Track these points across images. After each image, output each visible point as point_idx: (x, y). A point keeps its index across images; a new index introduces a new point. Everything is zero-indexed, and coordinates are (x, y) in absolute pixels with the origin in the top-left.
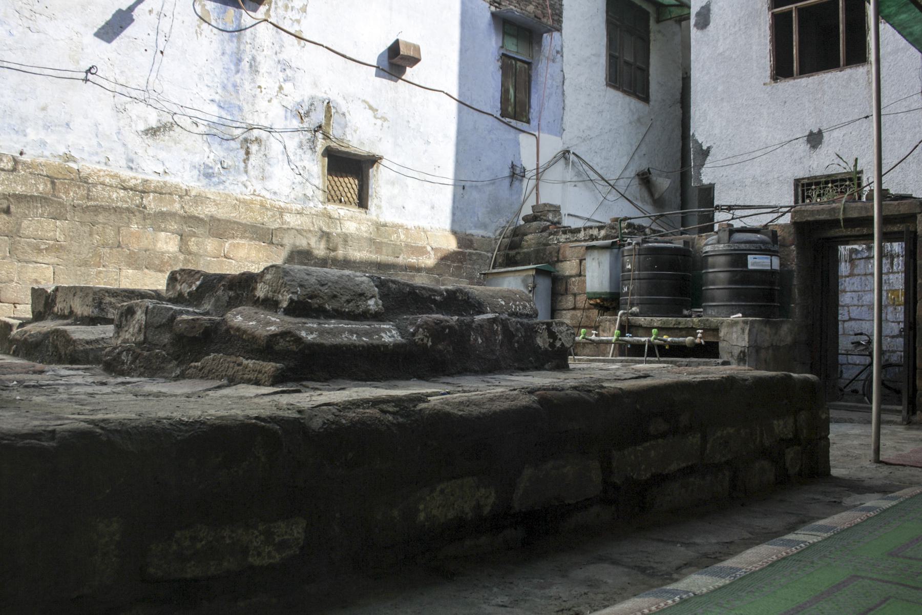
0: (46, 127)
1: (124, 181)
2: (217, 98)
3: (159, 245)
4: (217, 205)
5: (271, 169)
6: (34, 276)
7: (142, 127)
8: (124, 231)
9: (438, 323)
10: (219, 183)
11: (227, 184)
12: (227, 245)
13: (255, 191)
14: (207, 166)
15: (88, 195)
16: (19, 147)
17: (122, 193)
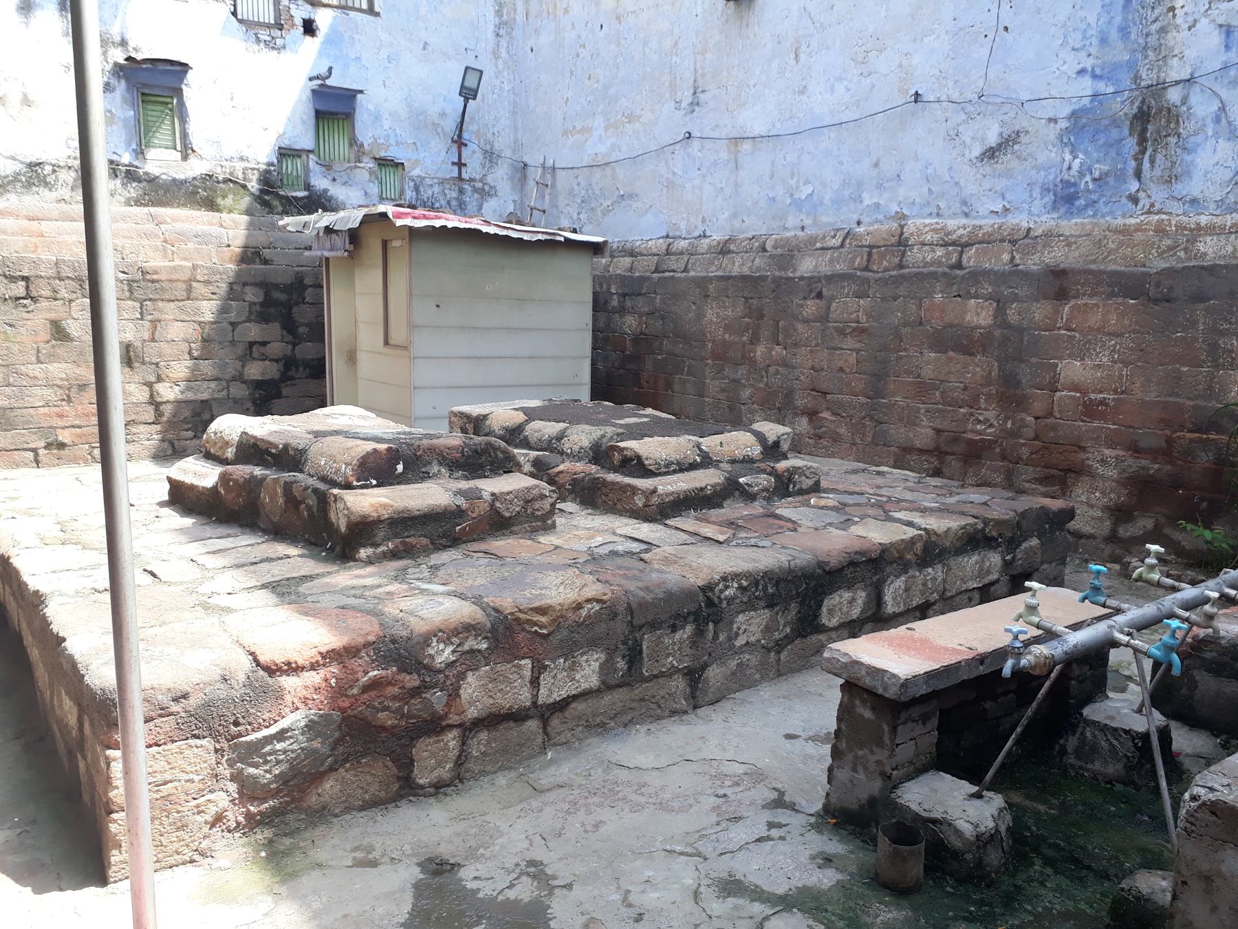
0: (879, 186)
1: (947, 234)
2: (1088, 63)
3: (968, 318)
5: (1189, 158)
6: (840, 364)
7: (977, 151)
10: (1086, 206)
11: (1101, 204)
13: (1152, 205)
14: (1067, 184)
15: (901, 260)
16: (855, 217)
17: (940, 252)
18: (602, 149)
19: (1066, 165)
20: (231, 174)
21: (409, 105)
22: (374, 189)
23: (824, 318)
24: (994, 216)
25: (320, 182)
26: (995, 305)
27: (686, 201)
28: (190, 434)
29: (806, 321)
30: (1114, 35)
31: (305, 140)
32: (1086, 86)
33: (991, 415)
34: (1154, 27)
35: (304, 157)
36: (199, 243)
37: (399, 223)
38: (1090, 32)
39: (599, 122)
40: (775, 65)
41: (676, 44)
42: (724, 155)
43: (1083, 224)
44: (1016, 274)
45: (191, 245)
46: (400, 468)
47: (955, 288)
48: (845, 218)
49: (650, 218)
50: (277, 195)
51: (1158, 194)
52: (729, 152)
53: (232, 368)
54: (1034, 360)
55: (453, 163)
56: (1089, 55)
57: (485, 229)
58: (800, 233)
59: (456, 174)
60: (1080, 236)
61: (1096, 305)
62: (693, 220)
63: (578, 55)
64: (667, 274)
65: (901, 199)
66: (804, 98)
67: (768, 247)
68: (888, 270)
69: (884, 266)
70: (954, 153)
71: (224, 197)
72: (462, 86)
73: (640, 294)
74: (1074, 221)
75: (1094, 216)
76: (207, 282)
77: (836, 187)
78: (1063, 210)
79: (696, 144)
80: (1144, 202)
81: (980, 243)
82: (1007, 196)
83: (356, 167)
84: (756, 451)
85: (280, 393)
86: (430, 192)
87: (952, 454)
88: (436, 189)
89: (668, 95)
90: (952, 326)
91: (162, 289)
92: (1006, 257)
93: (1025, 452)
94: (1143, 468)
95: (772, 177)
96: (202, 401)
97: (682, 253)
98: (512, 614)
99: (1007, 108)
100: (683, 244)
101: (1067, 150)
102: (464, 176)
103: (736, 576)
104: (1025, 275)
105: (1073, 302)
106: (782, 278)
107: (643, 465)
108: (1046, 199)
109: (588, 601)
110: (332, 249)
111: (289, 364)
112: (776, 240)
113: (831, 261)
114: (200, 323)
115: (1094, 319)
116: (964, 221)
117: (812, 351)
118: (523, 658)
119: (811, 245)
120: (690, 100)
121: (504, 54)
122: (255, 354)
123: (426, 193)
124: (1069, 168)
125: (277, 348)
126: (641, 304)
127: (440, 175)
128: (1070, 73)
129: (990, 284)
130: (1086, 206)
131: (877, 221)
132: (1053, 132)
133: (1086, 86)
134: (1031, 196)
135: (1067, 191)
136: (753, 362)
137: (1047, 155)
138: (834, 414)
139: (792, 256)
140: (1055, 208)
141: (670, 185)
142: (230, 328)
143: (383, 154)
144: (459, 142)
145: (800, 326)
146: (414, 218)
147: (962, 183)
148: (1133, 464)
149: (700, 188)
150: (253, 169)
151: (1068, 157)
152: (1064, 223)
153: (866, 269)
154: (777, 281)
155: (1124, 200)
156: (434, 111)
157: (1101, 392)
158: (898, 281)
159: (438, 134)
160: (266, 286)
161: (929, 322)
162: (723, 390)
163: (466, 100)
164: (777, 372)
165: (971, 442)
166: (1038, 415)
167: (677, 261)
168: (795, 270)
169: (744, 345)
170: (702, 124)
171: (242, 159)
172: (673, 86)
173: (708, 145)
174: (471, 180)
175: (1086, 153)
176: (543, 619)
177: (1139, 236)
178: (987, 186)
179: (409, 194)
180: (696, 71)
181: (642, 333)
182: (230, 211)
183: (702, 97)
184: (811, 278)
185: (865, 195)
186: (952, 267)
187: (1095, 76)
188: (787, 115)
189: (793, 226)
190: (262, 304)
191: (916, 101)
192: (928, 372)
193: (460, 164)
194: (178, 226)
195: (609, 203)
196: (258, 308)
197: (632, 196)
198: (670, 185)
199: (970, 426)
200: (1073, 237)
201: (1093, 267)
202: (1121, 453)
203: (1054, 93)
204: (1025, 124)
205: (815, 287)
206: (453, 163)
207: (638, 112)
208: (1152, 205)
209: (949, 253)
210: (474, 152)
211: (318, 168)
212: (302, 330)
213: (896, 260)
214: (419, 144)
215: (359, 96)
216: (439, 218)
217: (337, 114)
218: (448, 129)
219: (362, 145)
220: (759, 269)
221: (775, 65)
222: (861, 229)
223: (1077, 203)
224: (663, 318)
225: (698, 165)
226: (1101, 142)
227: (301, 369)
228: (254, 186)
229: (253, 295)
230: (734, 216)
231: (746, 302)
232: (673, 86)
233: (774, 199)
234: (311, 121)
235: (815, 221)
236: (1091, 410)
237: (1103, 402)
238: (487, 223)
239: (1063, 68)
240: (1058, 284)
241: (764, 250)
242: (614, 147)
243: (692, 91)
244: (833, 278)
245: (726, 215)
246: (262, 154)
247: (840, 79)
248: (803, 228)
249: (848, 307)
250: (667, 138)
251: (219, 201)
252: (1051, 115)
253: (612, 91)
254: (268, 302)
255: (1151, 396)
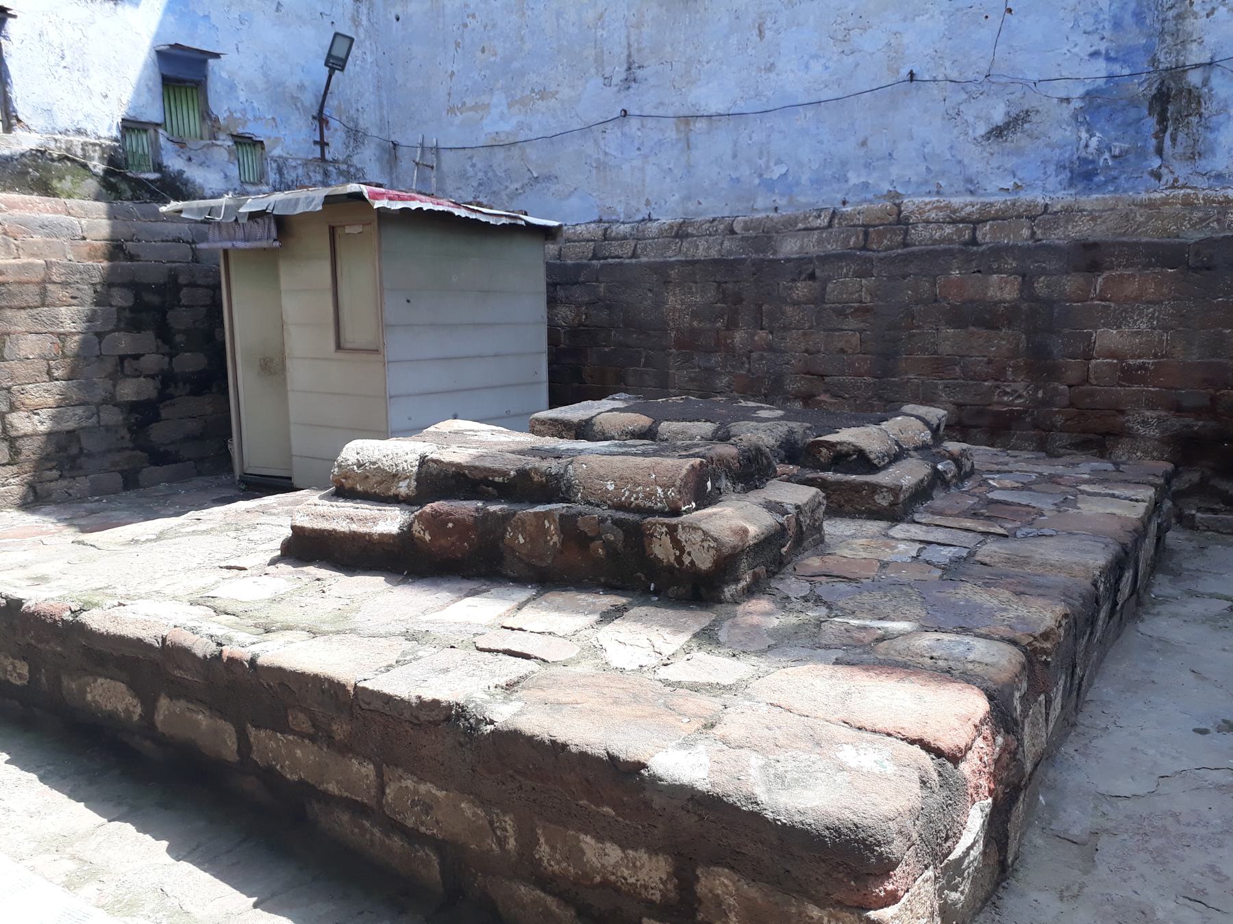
0: (867, 165)
1: (954, 212)
2: (1102, 46)
4: (1092, 219)
5: (1211, 136)
6: (841, 345)
7: (982, 130)
8: (941, 280)
9: (436, 515)
10: (1106, 183)
12: (1100, 280)
13: (1176, 180)
14: (1084, 161)
15: (904, 239)
16: (840, 197)
17: (949, 230)
18: (505, 127)
19: (1083, 143)
20: (68, 150)
21: (265, 75)
22: (234, 171)
23: (819, 299)
24: (1003, 193)
25: (174, 163)
26: (1020, 279)
27: (632, 187)
28: (55, 473)
29: (796, 303)
30: (1128, 19)
31: (153, 113)
32: (1100, 68)
33: (1020, 386)
34: (1171, 14)
35: (151, 131)
36: (48, 235)
37: (377, 204)
38: (1102, 17)
39: (499, 98)
40: (733, 40)
41: (601, 17)
42: (672, 134)
43: (1104, 199)
44: (1039, 249)
45: (37, 238)
47: (974, 264)
48: (830, 197)
49: (574, 202)
50: (125, 178)
51: (1182, 170)
52: (678, 130)
53: (102, 388)
54: (1067, 331)
55: (316, 143)
56: (1103, 38)
57: (457, 212)
58: (772, 214)
59: (318, 155)
60: (1104, 211)
61: (1133, 276)
62: (633, 203)
63: (465, 25)
64: (610, 260)
65: (894, 177)
66: (773, 75)
67: (737, 228)
68: (891, 249)
69: (883, 243)
70: (956, 132)
71: (61, 179)
72: (329, 55)
73: (576, 283)
74: (1094, 196)
75: (1116, 190)
76: (65, 284)
77: (815, 166)
78: (1080, 187)
79: (634, 123)
80: (1167, 178)
81: (993, 219)
82: (1019, 173)
83: (214, 145)
84: (927, 436)
85: (159, 414)
86: (294, 175)
87: (976, 427)
88: (300, 171)
89: (593, 71)
90: (972, 301)
91: (10, 293)
92: (1025, 232)
93: (1059, 420)
94: (1187, 426)
95: (735, 156)
96: (68, 432)
97: (625, 238)
98: (1030, 644)
99: (1012, 88)
100: (624, 229)
101: (1083, 129)
102: (328, 157)
104: (1052, 249)
105: (1106, 274)
106: (763, 260)
107: (868, 460)
108: (1062, 176)
110: (246, 240)
111: (166, 379)
112: (745, 222)
113: (820, 242)
114: (59, 335)
115: (1131, 288)
116: (969, 199)
117: (804, 334)
119: (789, 226)
120: (624, 76)
121: (365, 22)
122: (128, 370)
123: (290, 176)
124: (1087, 146)
125: (152, 361)
126: (578, 293)
127: (302, 155)
128: (1082, 55)
129: (1014, 259)
130: (1106, 183)
131: (865, 201)
132: (1066, 112)
133: (1100, 68)
134: (1045, 173)
135: (1084, 169)
136: (730, 350)
137: (1060, 133)
138: (835, 396)
139: (770, 238)
140: (1071, 183)
141: (601, 166)
142: (96, 340)
143: (240, 130)
144: (321, 119)
145: (789, 310)
146: (390, 199)
147: (966, 161)
148: (1177, 423)
149: (642, 170)
150: (94, 145)
151: (1084, 135)
152: (1084, 198)
153: (864, 248)
154: (759, 265)
155: (1146, 176)
156: (292, 82)
157: (1140, 357)
158: (906, 259)
159: (298, 109)
160: (135, 287)
161: (945, 298)
162: (692, 380)
163: (332, 71)
164: (762, 358)
165: (998, 414)
166: (1073, 382)
167: (621, 246)
168: (775, 253)
169: (718, 331)
170: (643, 100)
171: (79, 132)
172: (599, 61)
173: (650, 123)
174: (335, 161)
175: (1102, 131)
176: (1047, 645)
177: (1166, 209)
178: (995, 163)
179: (272, 176)
180: (629, 45)
181: (580, 324)
182: (69, 197)
183: (640, 73)
184: (800, 259)
185: (851, 175)
186: (966, 244)
187: (1109, 59)
188: (752, 93)
189: (762, 207)
190: (131, 309)
191: (912, 80)
192: (946, 348)
193: (322, 144)
194: (17, 213)
195: (518, 185)
196: (127, 314)
197: (548, 178)
198: (601, 166)
199: (996, 398)
200: (1096, 211)
201: (1124, 239)
202: (1163, 413)
203: (1065, 74)
204: (1035, 104)
205: (804, 268)
206: (316, 143)
207: (553, 88)
208: (1176, 180)
209: (959, 231)
210: (336, 130)
211: (169, 145)
212: (179, 338)
213: (900, 239)
214: (278, 120)
215: (211, 62)
216: (413, 199)
217: (184, 81)
218: (307, 104)
219: (217, 120)
220: (730, 252)
221: (733, 40)
222: (848, 209)
223: (1096, 179)
224: (609, 307)
225: (636, 144)
226: (1118, 121)
227: (181, 384)
228: (99, 167)
229: (121, 298)
230: (688, 198)
231: (718, 288)
232: (599, 61)
233: (738, 180)
234: (158, 89)
235: (790, 202)
236: (1129, 375)
237: (1142, 367)
238: (457, 205)
239: (1073, 50)
240: (1090, 257)
241: (732, 232)
242: (521, 126)
243: (625, 66)
244: (825, 259)
245: (677, 197)
246: (106, 128)
247: (815, 57)
248: (776, 209)
249: (846, 286)
250: (594, 117)
251: (55, 183)
252: (1063, 95)
253: (516, 65)
254: (138, 307)
255: (1194, 358)
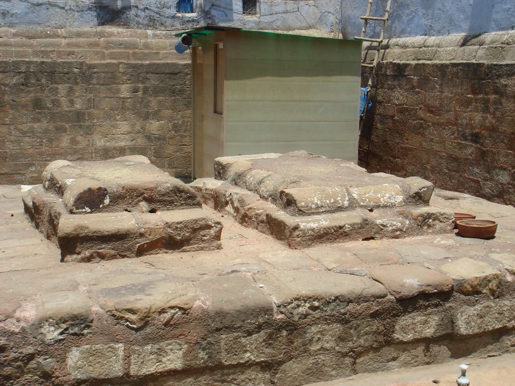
46: (107, 201)
103: (307, 299)
109: (172, 308)
118: (118, 342)
